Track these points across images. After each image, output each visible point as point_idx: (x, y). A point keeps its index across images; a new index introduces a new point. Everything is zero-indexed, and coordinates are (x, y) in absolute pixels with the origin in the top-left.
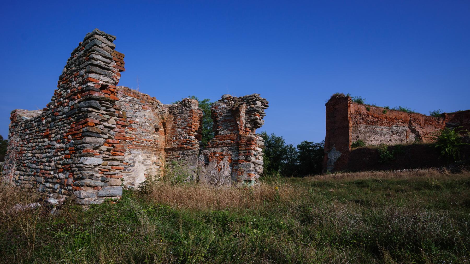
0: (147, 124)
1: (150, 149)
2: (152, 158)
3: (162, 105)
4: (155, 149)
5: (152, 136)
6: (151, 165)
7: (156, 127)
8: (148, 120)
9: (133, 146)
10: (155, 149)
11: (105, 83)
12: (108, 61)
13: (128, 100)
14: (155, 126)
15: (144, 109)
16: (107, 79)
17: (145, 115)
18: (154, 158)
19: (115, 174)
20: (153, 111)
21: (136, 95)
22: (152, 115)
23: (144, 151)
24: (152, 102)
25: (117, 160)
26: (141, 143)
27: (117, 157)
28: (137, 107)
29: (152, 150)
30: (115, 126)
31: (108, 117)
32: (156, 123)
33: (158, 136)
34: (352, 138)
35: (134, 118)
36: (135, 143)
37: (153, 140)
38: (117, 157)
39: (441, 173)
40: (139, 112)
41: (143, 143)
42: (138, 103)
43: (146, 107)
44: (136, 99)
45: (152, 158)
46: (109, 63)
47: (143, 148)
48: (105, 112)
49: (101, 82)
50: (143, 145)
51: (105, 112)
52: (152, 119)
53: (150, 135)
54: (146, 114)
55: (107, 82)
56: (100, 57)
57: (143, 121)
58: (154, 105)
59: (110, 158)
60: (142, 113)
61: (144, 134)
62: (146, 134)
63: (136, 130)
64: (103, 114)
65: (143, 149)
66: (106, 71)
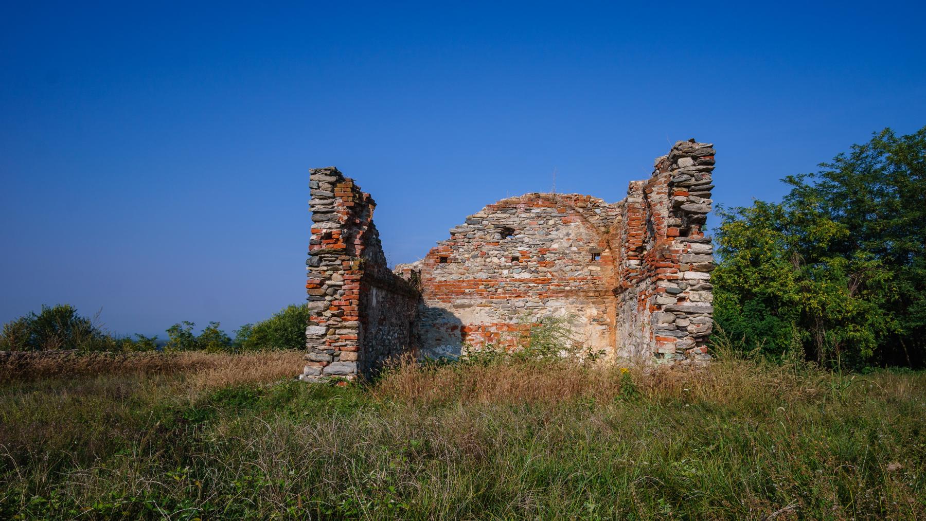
0: (574, 249)
1: (582, 294)
2: (588, 311)
3: (607, 205)
4: (592, 294)
5: (586, 270)
6: (586, 325)
7: (593, 252)
8: (575, 241)
9: (549, 294)
10: (592, 294)
11: (329, 231)
12: (329, 201)
13: (533, 215)
14: (592, 249)
15: (566, 223)
16: (329, 225)
17: (568, 234)
18: (594, 312)
19: (346, 345)
20: (585, 220)
21: (551, 202)
22: (583, 230)
23: (571, 299)
24: (584, 205)
25: (345, 327)
26: (565, 286)
27: (346, 324)
28: (551, 222)
29: (587, 297)
30: (342, 283)
31: (331, 272)
32: (592, 245)
33: (599, 269)
34: (693, 226)
35: (548, 244)
36: (551, 287)
37: (589, 277)
38: (346, 324)
39: (744, 357)
40: (557, 230)
41: (568, 285)
42: (553, 214)
43: (568, 218)
44: (549, 209)
45: (588, 311)
46: (332, 203)
47: (568, 294)
48: (325, 268)
49: (324, 231)
50: (568, 288)
51: (325, 268)
52: (584, 237)
53: (582, 269)
54: (570, 232)
55: (330, 228)
56: (317, 201)
57: (566, 245)
58: (587, 209)
59: (340, 325)
60: (563, 230)
61: (568, 268)
62: (573, 267)
63: (552, 264)
64: (325, 271)
65: (567, 296)
66: (329, 215)
